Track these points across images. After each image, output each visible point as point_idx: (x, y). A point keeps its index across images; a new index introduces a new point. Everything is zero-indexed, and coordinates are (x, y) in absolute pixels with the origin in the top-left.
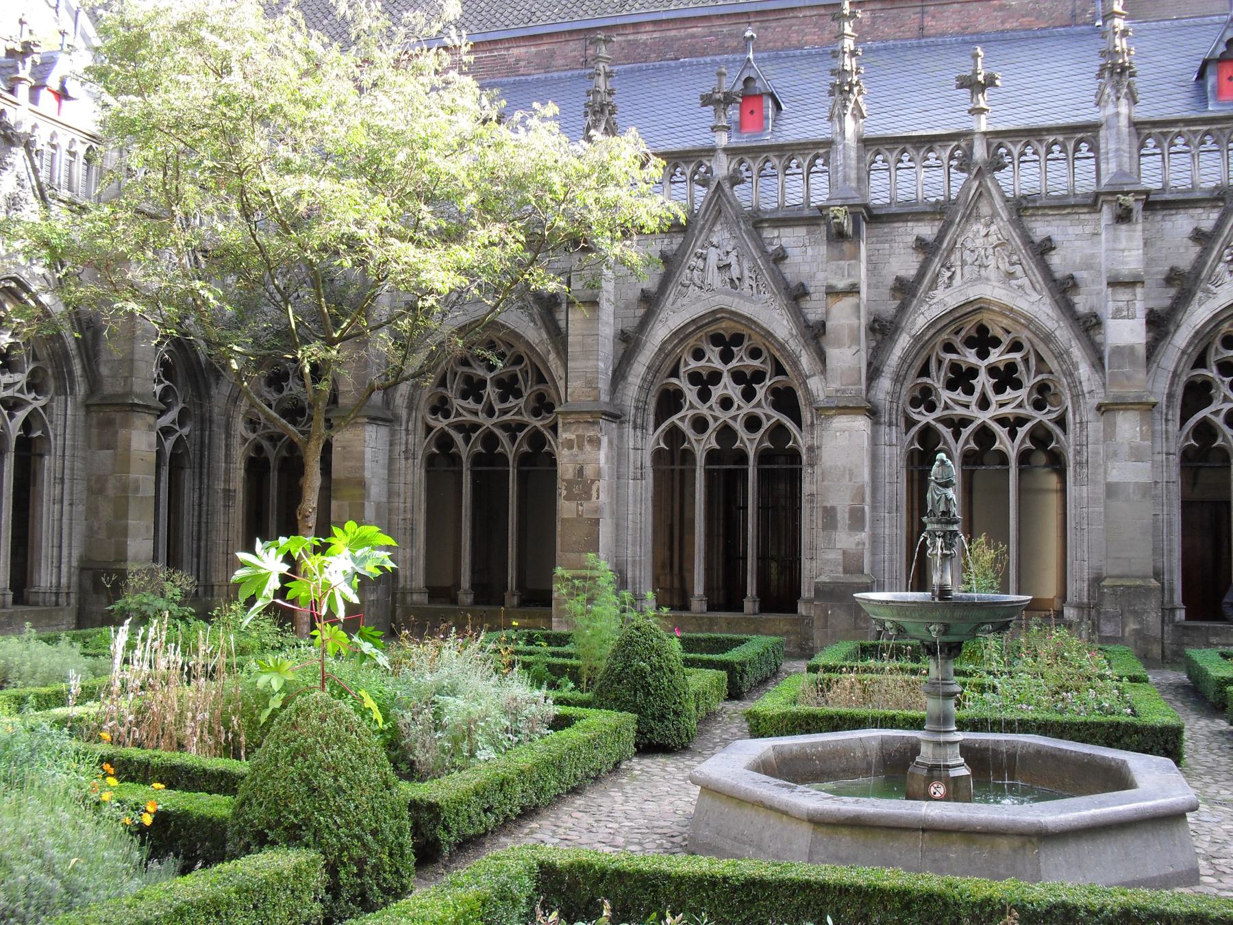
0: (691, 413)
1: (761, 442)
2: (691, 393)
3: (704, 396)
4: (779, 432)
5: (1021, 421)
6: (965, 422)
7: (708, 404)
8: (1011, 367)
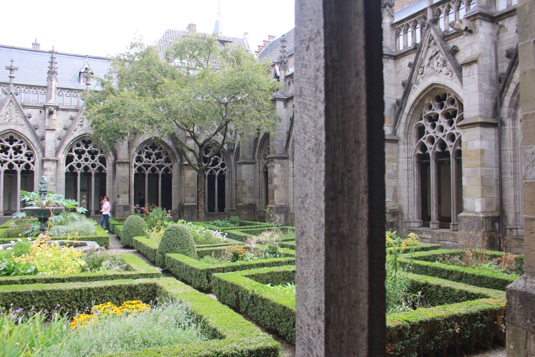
0: (77, 162)
1: (96, 171)
2: (76, 156)
3: (80, 157)
4: (100, 169)
5: (163, 166)
6: (149, 166)
7: (81, 160)
8: (160, 153)
